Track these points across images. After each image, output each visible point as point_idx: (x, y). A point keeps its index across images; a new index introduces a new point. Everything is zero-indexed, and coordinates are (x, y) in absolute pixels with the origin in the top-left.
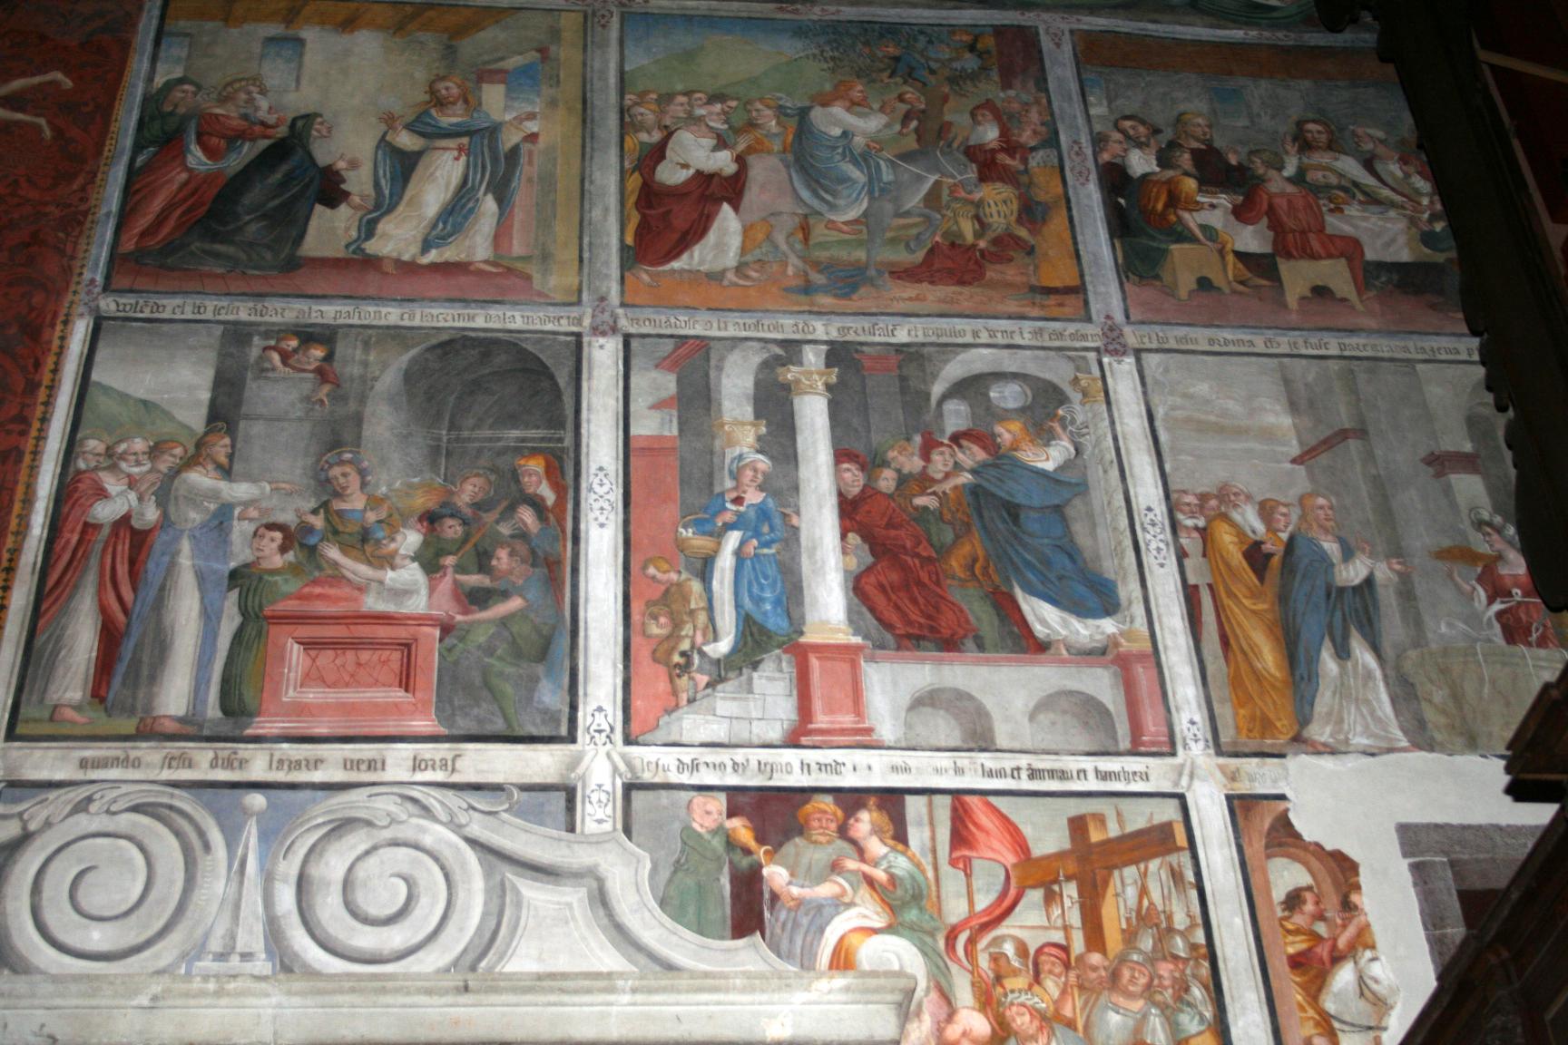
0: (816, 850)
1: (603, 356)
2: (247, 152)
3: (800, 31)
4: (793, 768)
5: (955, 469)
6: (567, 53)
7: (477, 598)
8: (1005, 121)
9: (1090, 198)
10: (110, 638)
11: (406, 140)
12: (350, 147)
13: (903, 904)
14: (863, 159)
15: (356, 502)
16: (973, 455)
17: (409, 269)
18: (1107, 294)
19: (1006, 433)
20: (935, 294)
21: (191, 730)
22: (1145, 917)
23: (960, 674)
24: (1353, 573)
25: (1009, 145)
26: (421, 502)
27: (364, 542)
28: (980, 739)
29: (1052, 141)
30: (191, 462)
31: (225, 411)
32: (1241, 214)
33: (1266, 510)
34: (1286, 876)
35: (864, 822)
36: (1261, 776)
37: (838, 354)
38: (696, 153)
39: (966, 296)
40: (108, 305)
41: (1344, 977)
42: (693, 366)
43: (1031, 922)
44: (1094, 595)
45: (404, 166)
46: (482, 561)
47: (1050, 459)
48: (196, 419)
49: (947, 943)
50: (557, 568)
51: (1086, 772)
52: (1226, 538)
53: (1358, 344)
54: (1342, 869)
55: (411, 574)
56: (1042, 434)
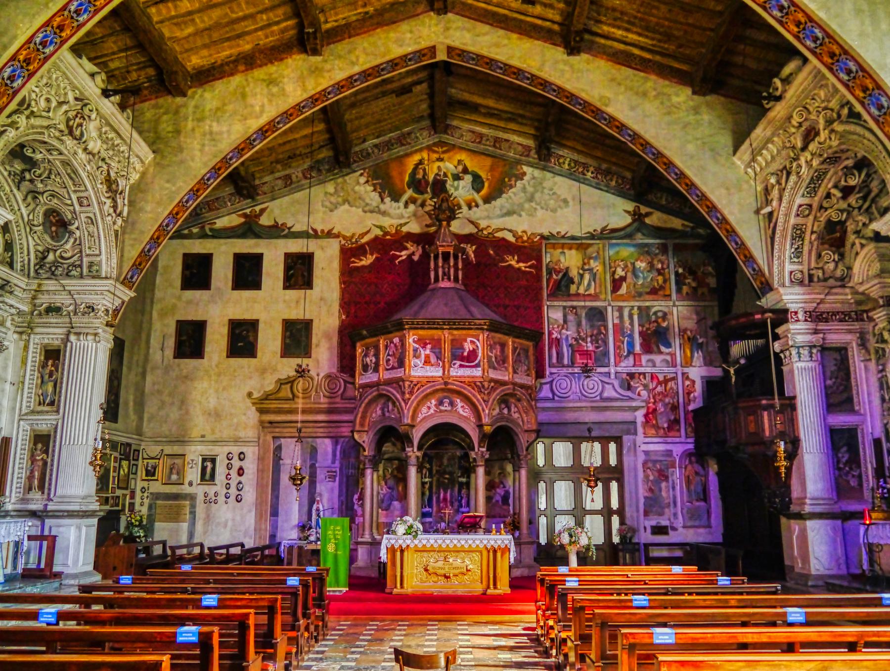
0: (636, 380)
1: (609, 309)
2: (561, 275)
3: (635, 246)
4: (633, 370)
5: (653, 326)
6: (601, 253)
7: (597, 348)
8: (663, 263)
9: (673, 277)
10: (558, 354)
11: (581, 272)
12: (574, 273)
13: (645, 386)
14: (642, 273)
15: (582, 334)
16: (655, 324)
17: (584, 295)
18: (674, 296)
19: (660, 320)
20: (651, 297)
21: (568, 366)
22: (671, 388)
23: (652, 357)
24: (700, 341)
25: (663, 269)
26: (589, 334)
27: (583, 340)
28: (654, 366)
29: (668, 267)
30: (563, 328)
31: (565, 321)
32: (694, 280)
33: (691, 332)
34: (687, 383)
35: (641, 377)
36: (686, 370)
37: (639, 308)
38: (620, 272)
39: (655, 297)
40: (548, 303)
41: (692, 395)
42: (620, 309)
43: (659, 389)
44: (668, 345)
45: (582, 276)
46: (597, 342)
47: (665, 324)
48: (561, 322)
49: (650, 391)
50: (606, 343)
51: (666, 370)
52: (686, 337)
53: (707, 303)
54: (693, 382)
55: (589, 344)
56: (664, 321)
